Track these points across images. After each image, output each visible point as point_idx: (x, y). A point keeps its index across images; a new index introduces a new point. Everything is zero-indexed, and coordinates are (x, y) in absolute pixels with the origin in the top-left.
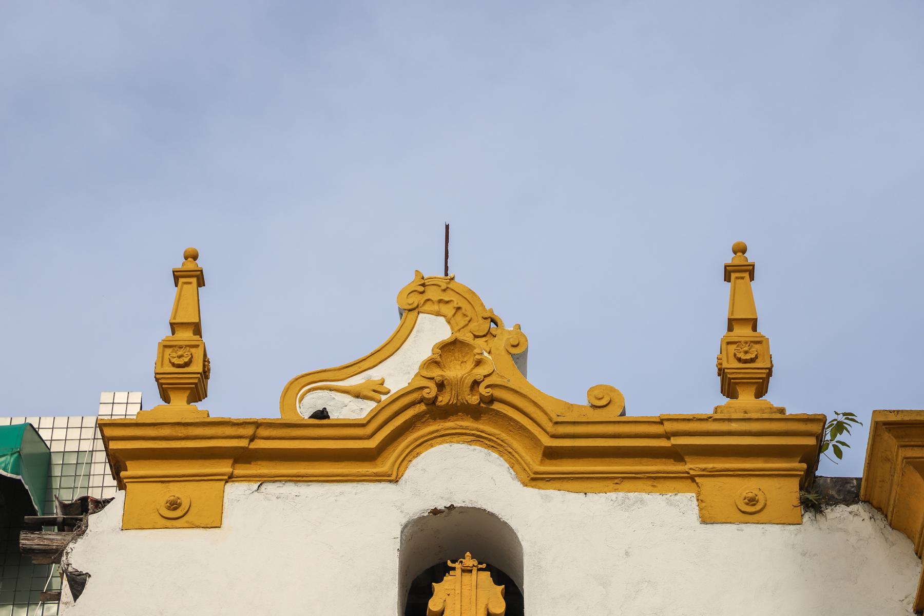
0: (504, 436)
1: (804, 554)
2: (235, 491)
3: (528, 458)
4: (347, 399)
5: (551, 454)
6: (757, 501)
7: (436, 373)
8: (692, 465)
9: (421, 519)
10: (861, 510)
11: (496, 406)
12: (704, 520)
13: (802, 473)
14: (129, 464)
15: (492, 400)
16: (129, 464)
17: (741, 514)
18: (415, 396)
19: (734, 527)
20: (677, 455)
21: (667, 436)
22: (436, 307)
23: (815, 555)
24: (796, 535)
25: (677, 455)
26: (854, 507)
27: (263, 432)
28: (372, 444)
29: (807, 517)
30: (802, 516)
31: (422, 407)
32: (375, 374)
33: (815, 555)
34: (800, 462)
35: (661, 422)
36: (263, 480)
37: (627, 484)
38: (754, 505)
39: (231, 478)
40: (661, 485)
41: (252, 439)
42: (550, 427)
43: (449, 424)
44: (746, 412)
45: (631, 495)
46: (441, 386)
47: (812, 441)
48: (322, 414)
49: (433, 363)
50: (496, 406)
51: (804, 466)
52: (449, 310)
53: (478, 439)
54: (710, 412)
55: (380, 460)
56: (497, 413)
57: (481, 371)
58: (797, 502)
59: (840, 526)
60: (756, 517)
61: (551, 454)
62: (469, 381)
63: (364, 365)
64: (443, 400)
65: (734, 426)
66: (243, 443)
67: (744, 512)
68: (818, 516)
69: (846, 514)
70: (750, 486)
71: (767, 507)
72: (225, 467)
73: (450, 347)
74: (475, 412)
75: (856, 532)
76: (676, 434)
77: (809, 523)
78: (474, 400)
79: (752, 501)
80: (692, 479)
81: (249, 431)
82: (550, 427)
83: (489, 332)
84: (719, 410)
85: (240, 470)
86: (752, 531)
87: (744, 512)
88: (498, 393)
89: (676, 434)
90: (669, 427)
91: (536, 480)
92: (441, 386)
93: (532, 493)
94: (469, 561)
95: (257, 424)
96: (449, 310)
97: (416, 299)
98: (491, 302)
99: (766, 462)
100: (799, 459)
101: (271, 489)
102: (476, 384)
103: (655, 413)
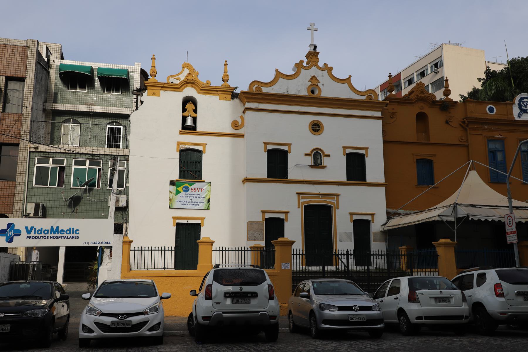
0: (195, 87)
2: (161, 92)
3: (198, 90)
4: (176, 80)
5: (201, 90)
7: (187, 78)
8: (219, 92)
9: (185, 97)
11: (195, 83)
12: (220, 100)
14: (148, 87)
15: (194, 82)
16: (148, 87)
18: (185, 81)
20: (217, 91)
21: (216, 89)
22: (187, 67)
25: (217, 91)
27: (165, 84)
28: (179, 87)
29: (232, 100)
31: (185, 82)
32: (179, 76)
35: (215, 87)
36: (165, 90)
37: (211, 94)
39: (161, 90)
40: (215, 95)
41: (164, 85)
42: (201, 86)
43: (189, 85)
45: (211, 96)
46: (188, 80)
48: (173, 82)
49: (187, 76)
50: (195, 83)
52: (189, 68)
53: (192, 87)
55: (180, 89)
56: (195, 84)
57: (193, 78)
61: (201, 90)
62: (191, 79)
63: (177, 75)
64: (188, 82)
65: (224, 88)
66: (163, 86)
70: (225, 96)
72: (160, 88)
73: (189, 74)
74: (192, 83)
76: (217, 89)
78: (192, 82)
79: (225, 98)
80: (219, 94)
81: (163, 84)
82: (201, 86)
83: (194, 72)
85: (162, 89)
86: (225, 101)
88: (195, 81)
89: (217, 89)
90: (216, 88)
91: (199, 93)
92: (188, 80)
93: (199, 95)
94: (191, 102)
95: (164, 83)
96: (189, 68)
97: (184, 66)
98: (194, 67)
101: (166, 91)
102: (192, 80)
103: (215, 86)
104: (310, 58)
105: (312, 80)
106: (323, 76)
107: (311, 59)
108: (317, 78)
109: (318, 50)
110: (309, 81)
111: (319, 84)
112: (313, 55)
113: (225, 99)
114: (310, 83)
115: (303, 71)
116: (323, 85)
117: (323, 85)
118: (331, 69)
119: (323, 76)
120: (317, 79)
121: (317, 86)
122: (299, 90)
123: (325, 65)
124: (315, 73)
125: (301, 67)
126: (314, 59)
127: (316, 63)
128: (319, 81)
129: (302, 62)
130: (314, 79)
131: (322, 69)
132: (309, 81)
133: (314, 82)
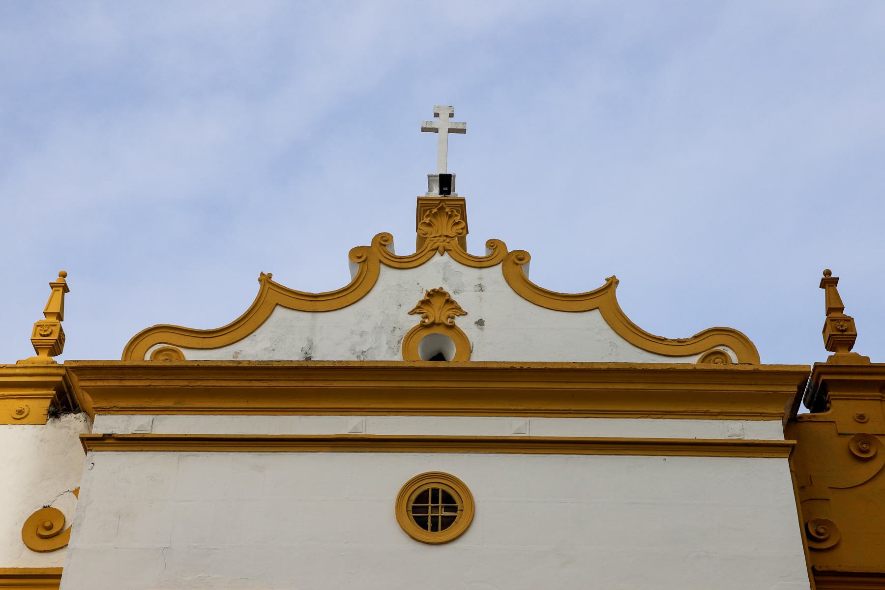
1: (41, 441)
6: (23, 412)
10: (81, 416)
13: (53, 396)
17: (13, 420)
19: (8, 426)
23: (48, 441)
24: (41, 430)
26: (78, 415)
29: (51, 419)
30: (48, 420)
33: (48, 441)
34: (54, 390)
38: (21, 414)
44: (33, 363)
47: (60, 379)
51: (54, 392)
54: (13, 362)
58: (46, 412)
59: (67, 425)
60: (21, 421)
67: (15, 418)
68: (56, 420)
69: (73, 418)
71: (28, 416)
75: (75, 428)
77: (50, 424)
79: (20, 412)
84: (19, 362)
86: (18, 428)
87: (15, 418)
99: (35, 391)
100: (53, 389)
104: (425, 223)
105: (426, 309)
106: (482, 290)
107: (426, 229)
108: (454, 297)
109: (460, 190)
110: (412, 313)
111: (459, 322)
112: (435, 210)
113: (20, 417)
114: (417, 320)
115: (388, 277)
116: (480, 323)
117: (480, 323)
118: (521, 258)
119: (482, 290)
120: (453, 302)
121: (452, 327)
122: (363, 352)
123: (493, 244)
124: (445, 279)
125: (381, 262)
126: (444, 226)
127: (448, 240)
128: (459, 308)
129: (384, 240)
130: (438, 302)
131: (479, 263)
132: (412, 313)
133: (437, 313)
